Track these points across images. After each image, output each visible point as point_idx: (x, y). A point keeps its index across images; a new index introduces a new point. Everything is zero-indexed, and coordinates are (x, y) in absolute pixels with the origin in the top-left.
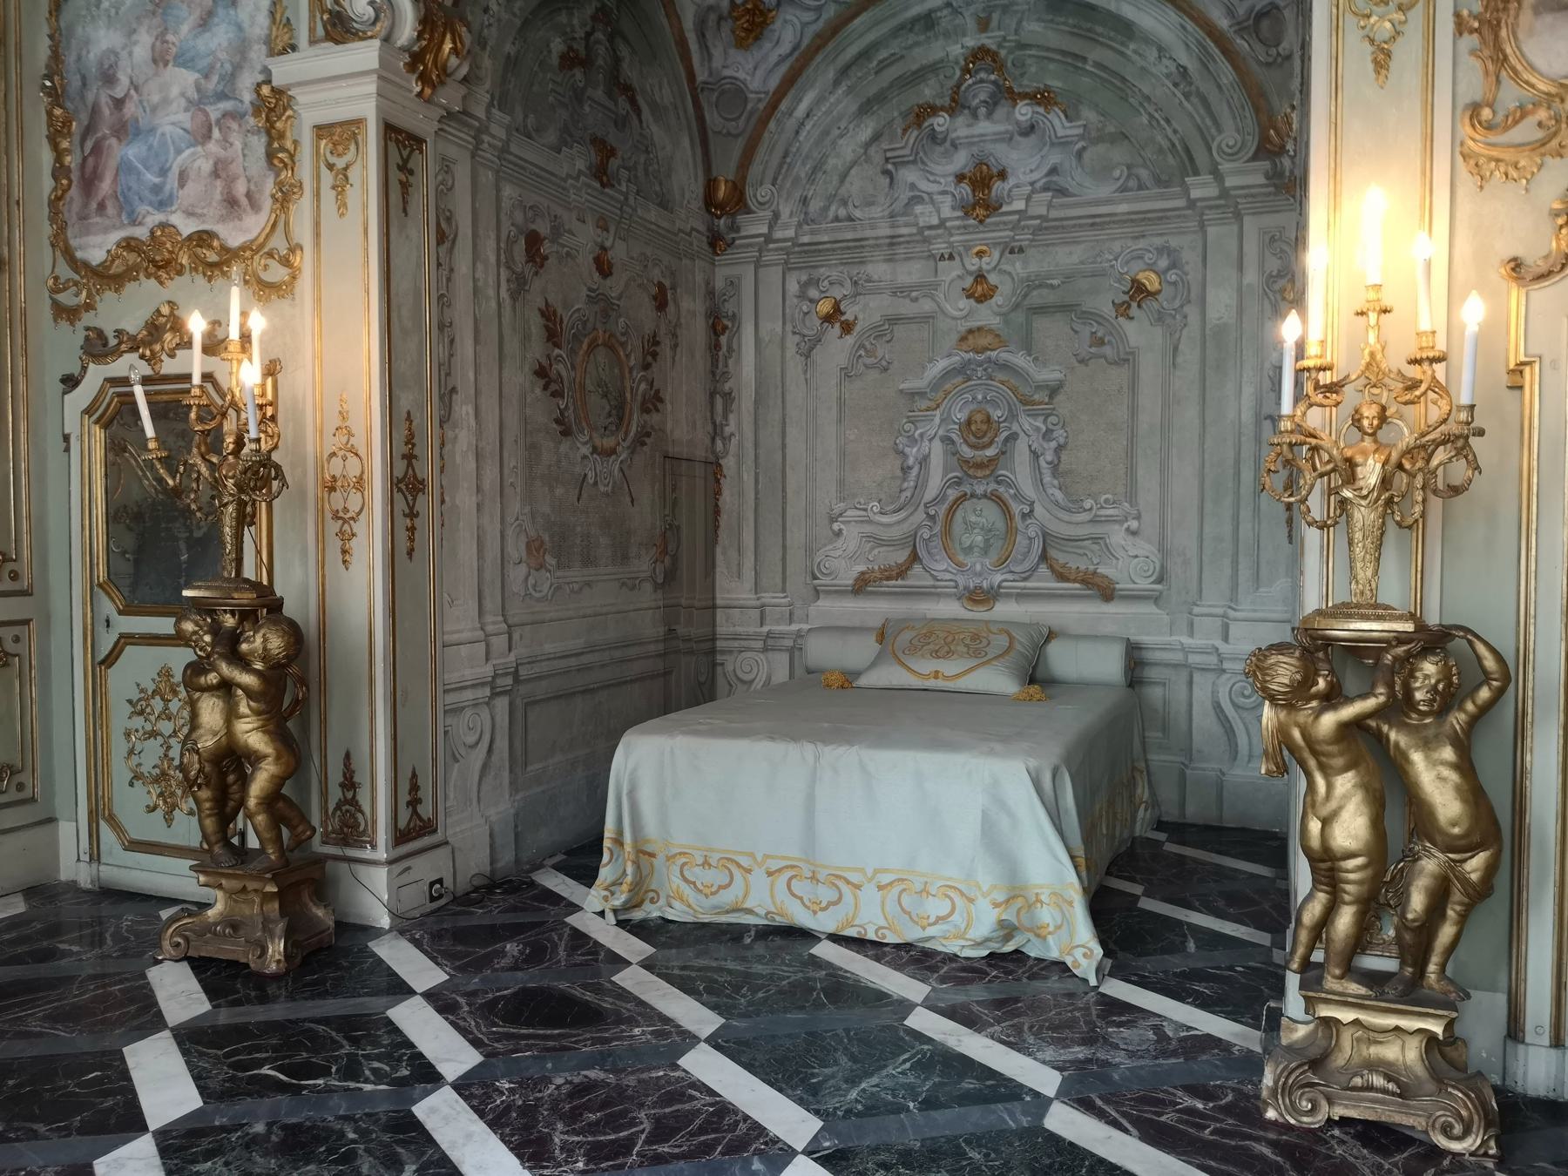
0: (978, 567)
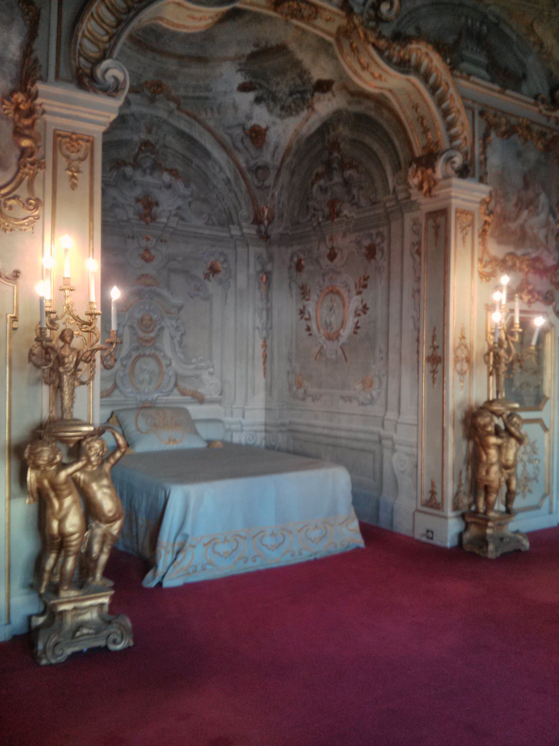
0: (147, 390)
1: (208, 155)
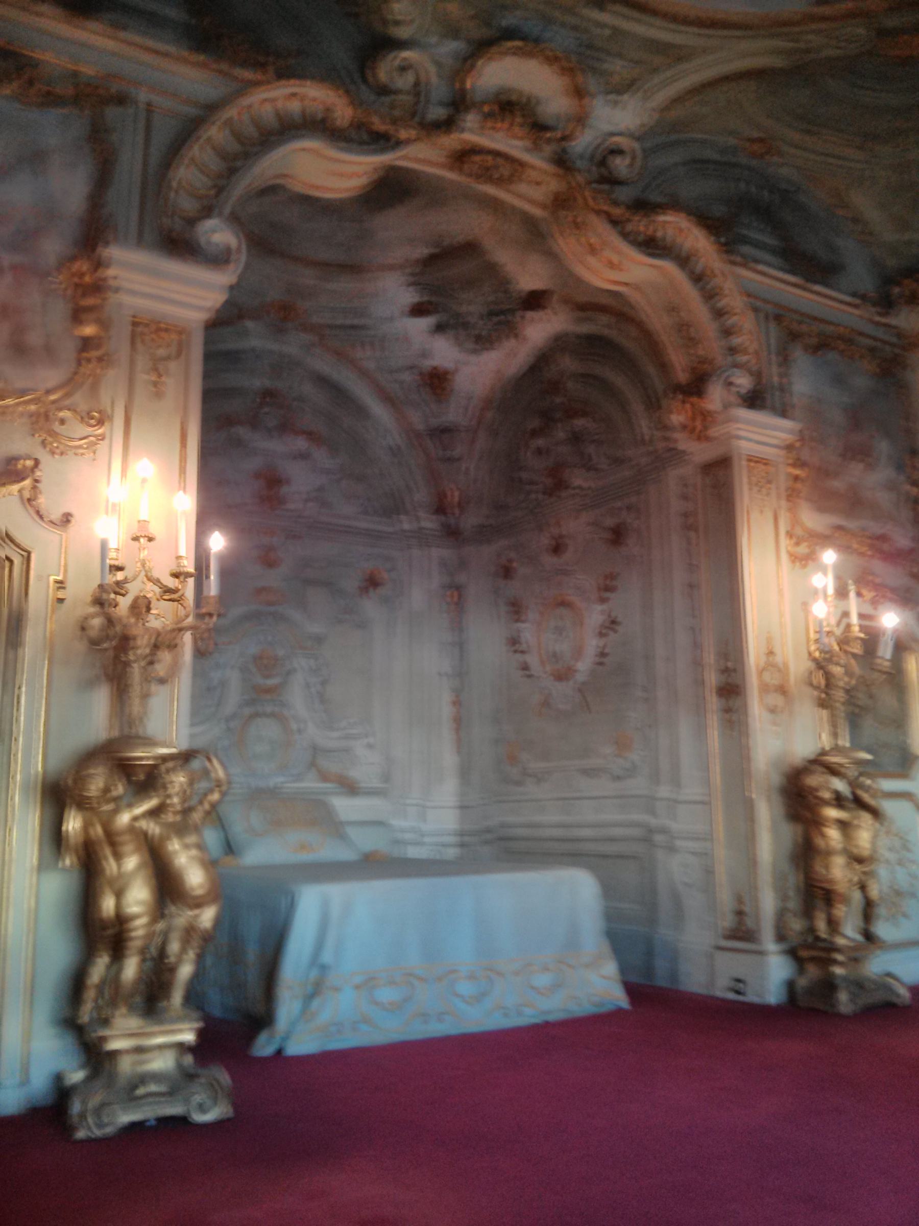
1: (361, 412)
